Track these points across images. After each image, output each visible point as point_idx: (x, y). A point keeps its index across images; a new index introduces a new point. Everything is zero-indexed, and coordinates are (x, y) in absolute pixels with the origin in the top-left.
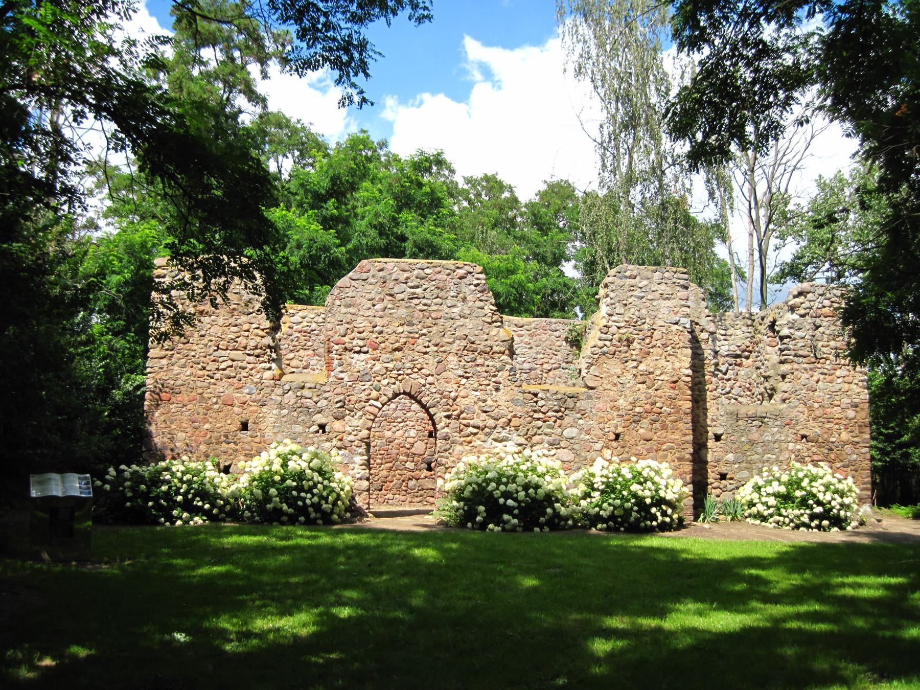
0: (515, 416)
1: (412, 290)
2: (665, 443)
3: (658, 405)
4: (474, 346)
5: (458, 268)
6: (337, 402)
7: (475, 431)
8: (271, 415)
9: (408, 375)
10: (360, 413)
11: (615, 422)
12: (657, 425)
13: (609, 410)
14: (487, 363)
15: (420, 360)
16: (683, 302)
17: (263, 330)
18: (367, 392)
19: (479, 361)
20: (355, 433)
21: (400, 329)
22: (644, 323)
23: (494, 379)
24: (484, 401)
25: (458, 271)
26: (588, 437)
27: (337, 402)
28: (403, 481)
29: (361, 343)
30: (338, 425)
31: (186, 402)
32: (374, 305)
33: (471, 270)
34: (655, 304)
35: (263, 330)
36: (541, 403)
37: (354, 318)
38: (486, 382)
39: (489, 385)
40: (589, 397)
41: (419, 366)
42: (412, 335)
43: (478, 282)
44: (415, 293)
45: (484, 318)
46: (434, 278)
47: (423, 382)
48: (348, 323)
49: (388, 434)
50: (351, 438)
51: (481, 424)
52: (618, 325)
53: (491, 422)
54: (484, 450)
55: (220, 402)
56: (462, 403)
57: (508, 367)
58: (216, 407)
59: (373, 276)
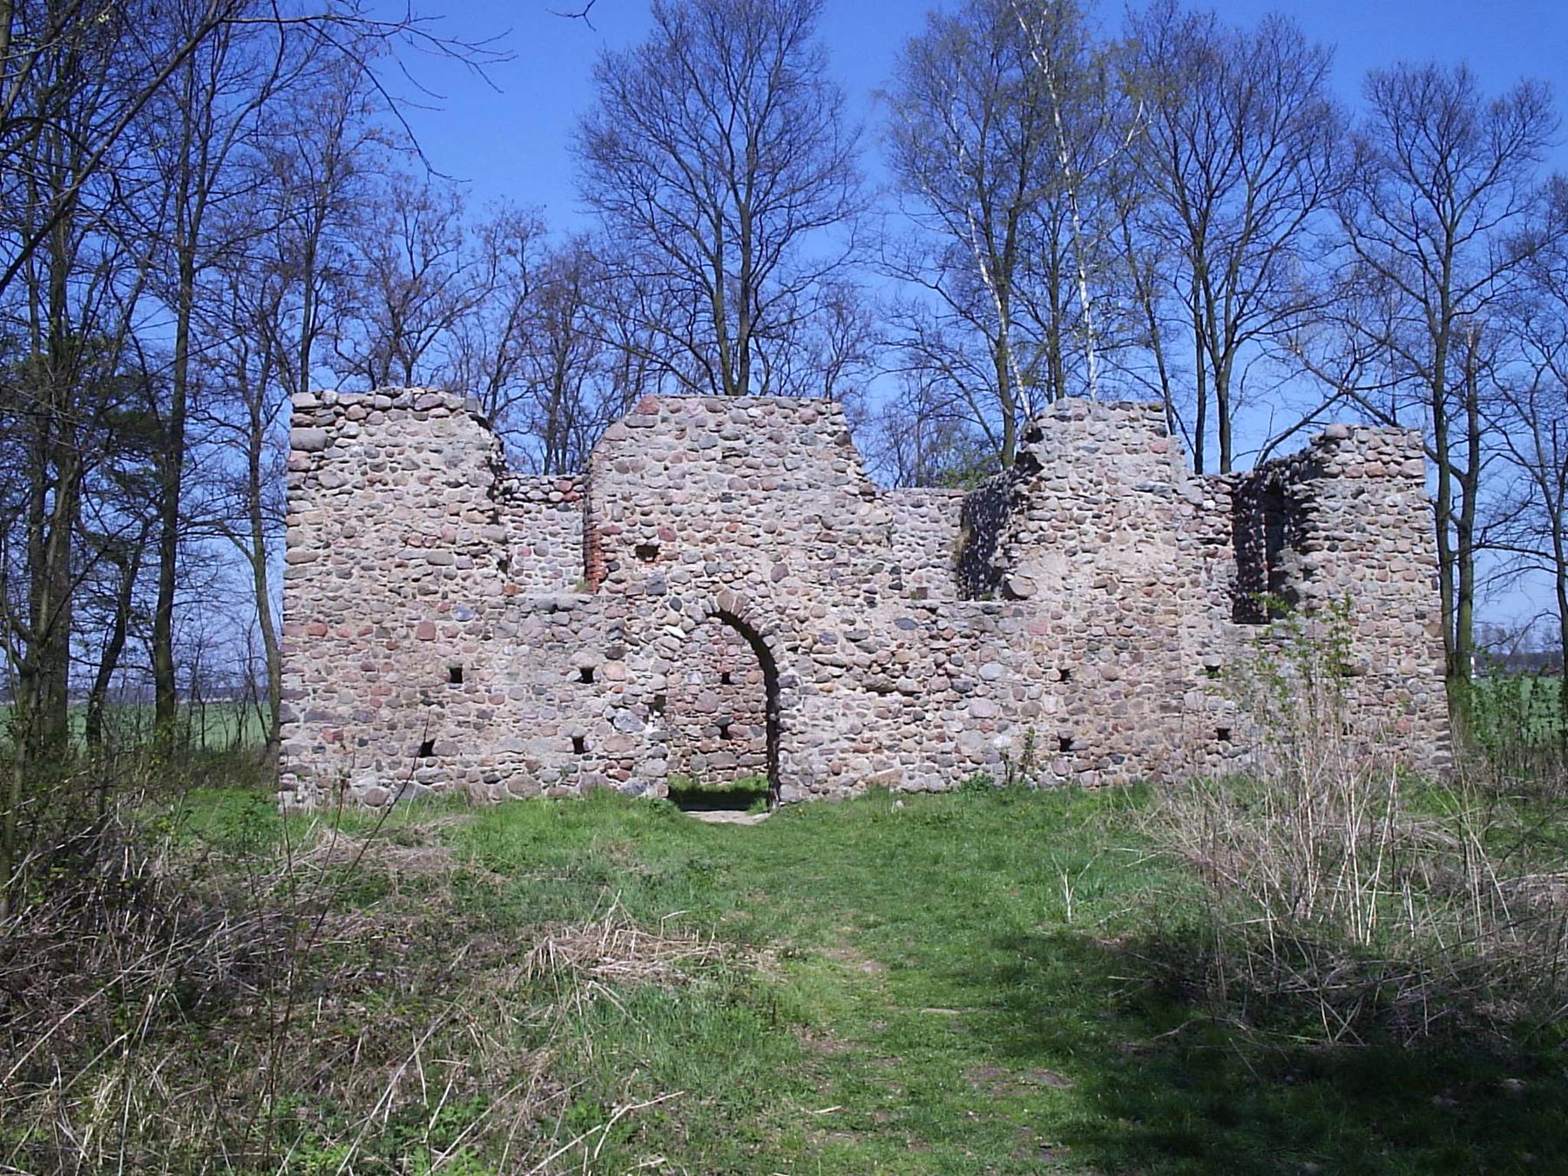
0: (901, 646)
1: (728, 444)
2: (1140, 683)
3: (1127, 622)
5: (801, 405)
6: (611, 631)
7: (837, 671)
8: (500, 655)
9: (726, 582)
11: (1060, 651)
12: (1125, 655)
13: (1049, 632)
14: (854, 560)
15: (747, 558)
16: (1161, 457)
17: (482, 512)
18: (660, 612)
19: (843, 558)
20: (642, 680)
21: (711, 508)
22: (1100, 491)
23: (865, 586)
24: (852, 623)
26: (1018, 676)
27: (611, 631)
28: (683, 756)
29: (647, 531)
30: (613, 669)
31: (353, 637)
34: (1116, 459)
35: (482, 512)
36: (942, 623)
38: (854, 592)
39: (858, 596)
40: (1018, 613)
41: (745, 568)
43: (836, 428)
44: (734, 449)
45: (846, 488)
47: (752, 593)
48: (624, 499)
50: (637, 689)
51: (846, 660)
52: (1060, 495)
53: (865, 658)
54: (854, 704)
55: (413, 635)
56: (816, 627)
57: (888, 566)
58: (406, 643)
59: (664, 420)
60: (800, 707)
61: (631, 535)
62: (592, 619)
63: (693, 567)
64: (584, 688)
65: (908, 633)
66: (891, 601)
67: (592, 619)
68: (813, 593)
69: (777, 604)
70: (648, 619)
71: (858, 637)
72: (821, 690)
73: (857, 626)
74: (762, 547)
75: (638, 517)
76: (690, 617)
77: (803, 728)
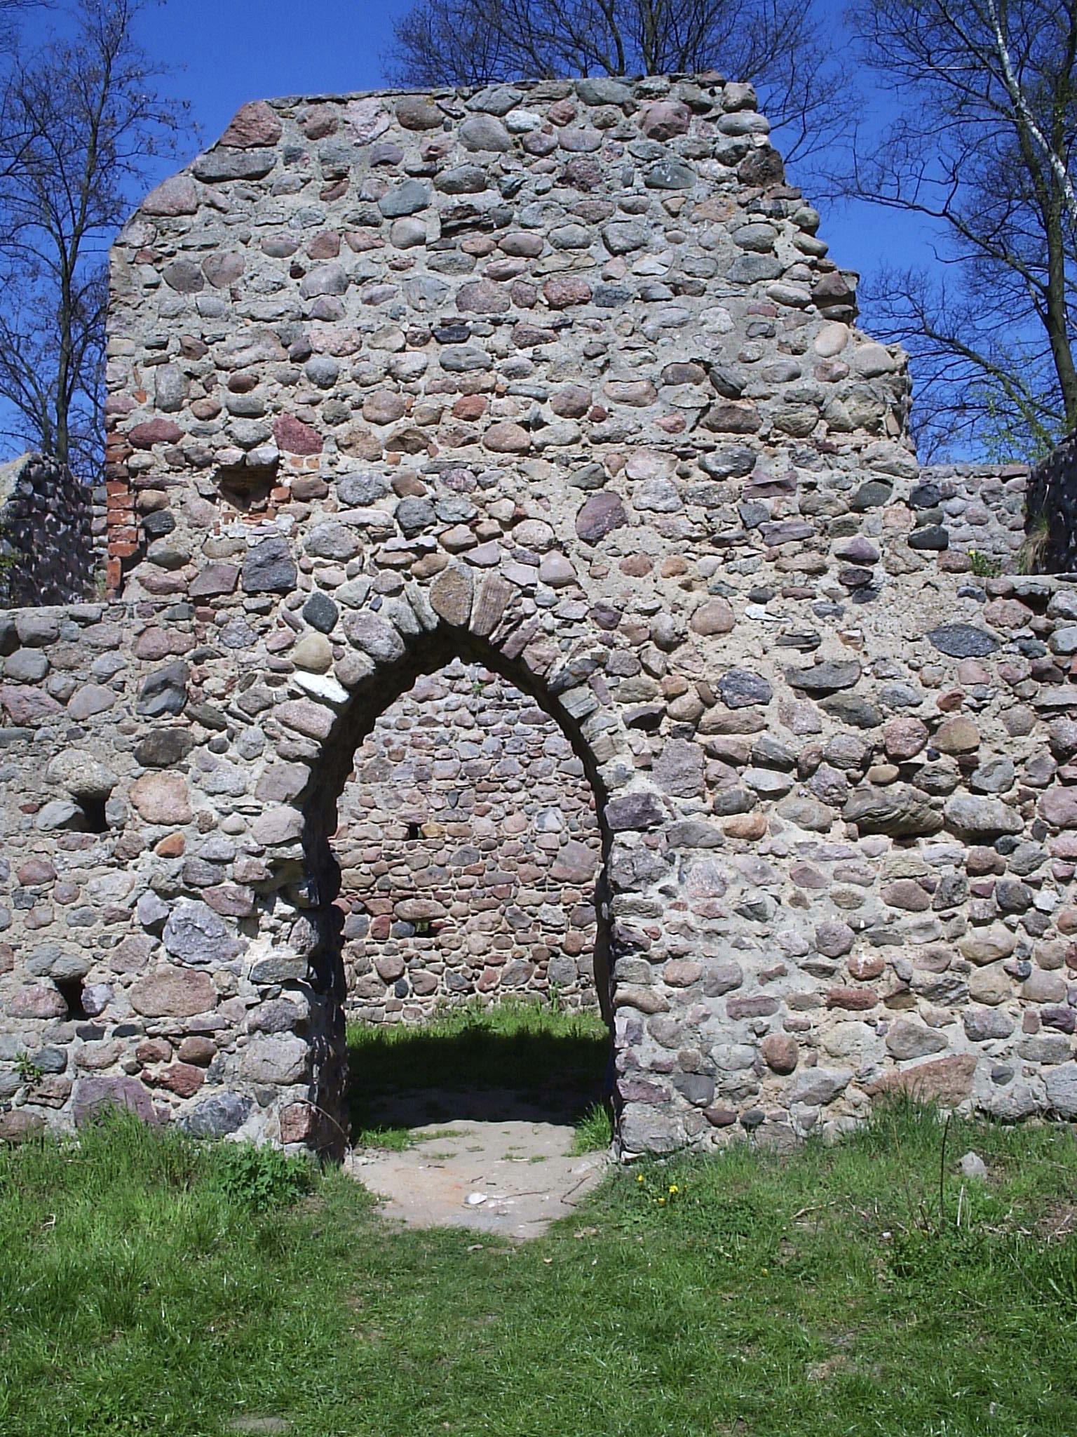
0: (952, 702)
1: (455, 200)
4: (741, 404)
7: (771, 780)
9: (455, 549)
10: (253, 733)
14: (805, 475)
18: (277, 637)
19: (774, 467)
20: (234, 821)
21: (412, 360)
23: (842, 544)
24: (809, 643)
25: (645, 104)
27: (151, 691)
28: (535, 960)
29: (244, 429)
32: (297, 272)
33: (704, 96)
37: (212, 328)
38: (810, 559)
39: (822, 571)
41: (505, 509)
42: (467, 378)
44: (470, 211)
45: (775, 286)
46: (552, 139)
47: (523, 574)
48: (187, 352)
49: (483, 825)
50: (220, 844)
51: (797, 747)
53: (852, 740)
54: (825, 870)
57: (903, 487)
59: (292, 156)
60: (670, 881)
61: (203, 442)
62: (103, 662)
63: (364, 514)
64: (82, 846)
65: (971, 667)
66: (916, 580)
67: (103, 662)
68: (696, 569)
69: (595, 597)
70: (245, 656)
71: (828, 681)
72: (729, 832)
73: (823, 651)
74: (548, 454)
75: (222, 396)
76: (357, 645)
77: (681, 942)
